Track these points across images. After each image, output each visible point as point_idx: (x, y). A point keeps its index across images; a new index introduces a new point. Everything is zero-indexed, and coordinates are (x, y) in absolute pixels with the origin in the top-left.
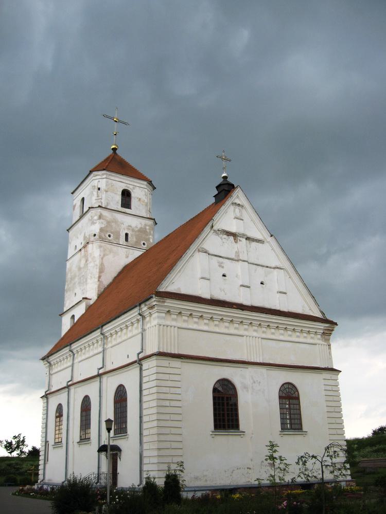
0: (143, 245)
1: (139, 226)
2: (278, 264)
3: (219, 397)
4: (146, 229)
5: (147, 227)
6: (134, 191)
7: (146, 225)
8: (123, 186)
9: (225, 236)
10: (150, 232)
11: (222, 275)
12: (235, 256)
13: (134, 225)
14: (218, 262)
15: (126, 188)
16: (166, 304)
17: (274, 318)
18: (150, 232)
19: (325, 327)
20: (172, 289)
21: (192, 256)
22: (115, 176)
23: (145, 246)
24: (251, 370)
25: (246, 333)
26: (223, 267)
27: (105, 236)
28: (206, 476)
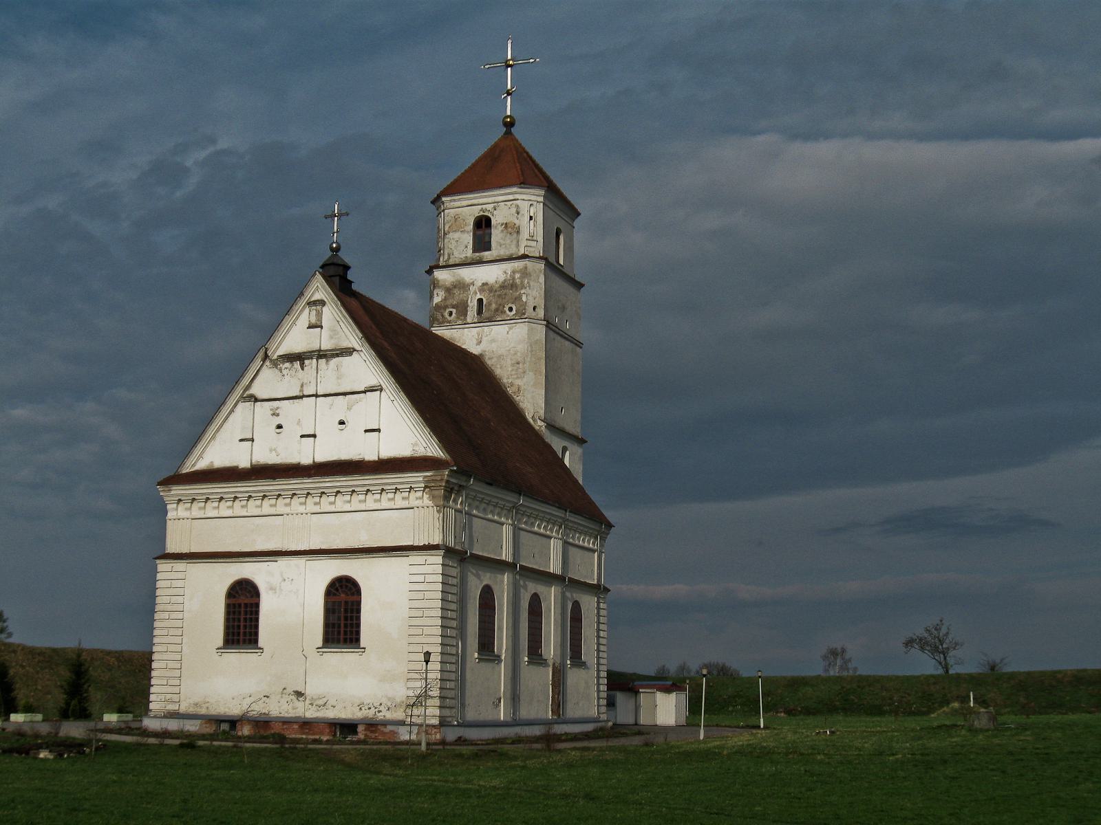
0: (508, 312)
1: (502, 278)
2: (373, 381)
3: (234, 605)
4: (514, 279)
5: (517, 276)
6: (495, 212)
7: (514, 272)
8: (476, 211)
9: (287, 365)
10: (522, 282)
11: (274, 426)
12: (300, 391)
13: (491, 280)
14: (271, 410)
15: (482, 213)
16: (172, 492)
17: (327, 480)
18: (522, 282)
19: (426, 477)
20: (202, 465)
21: (232, 411)
22: (459, 200)
23: (514, 312)
24: (283, 562)
25: (287, 510)
26: (278, 415)
27: (443, 316)
28: (208, 702)
